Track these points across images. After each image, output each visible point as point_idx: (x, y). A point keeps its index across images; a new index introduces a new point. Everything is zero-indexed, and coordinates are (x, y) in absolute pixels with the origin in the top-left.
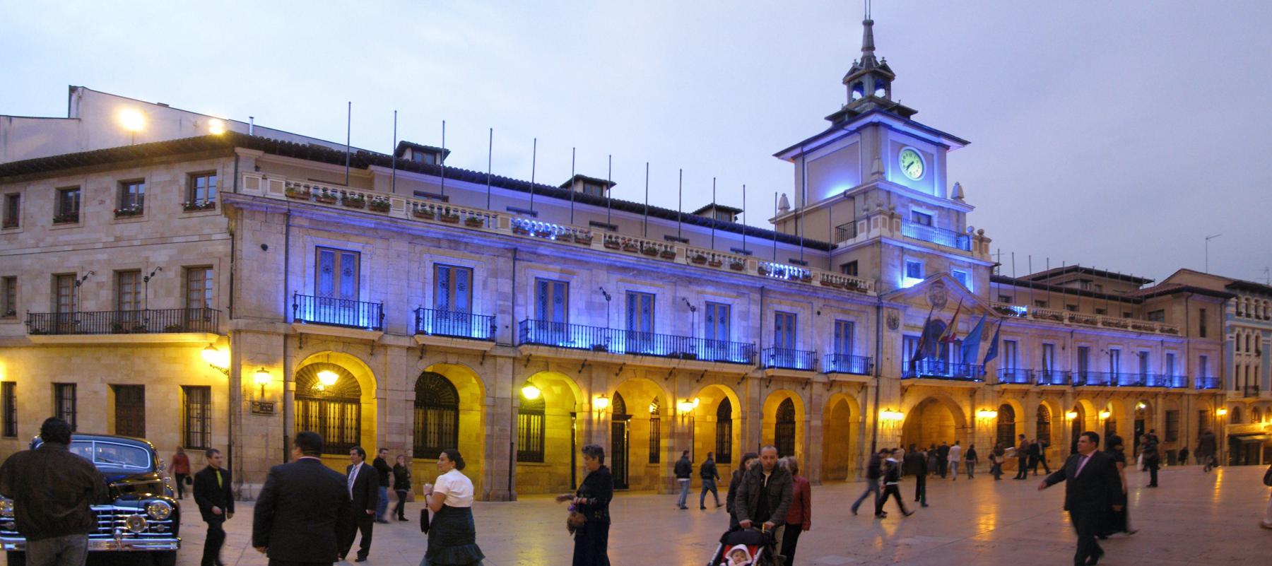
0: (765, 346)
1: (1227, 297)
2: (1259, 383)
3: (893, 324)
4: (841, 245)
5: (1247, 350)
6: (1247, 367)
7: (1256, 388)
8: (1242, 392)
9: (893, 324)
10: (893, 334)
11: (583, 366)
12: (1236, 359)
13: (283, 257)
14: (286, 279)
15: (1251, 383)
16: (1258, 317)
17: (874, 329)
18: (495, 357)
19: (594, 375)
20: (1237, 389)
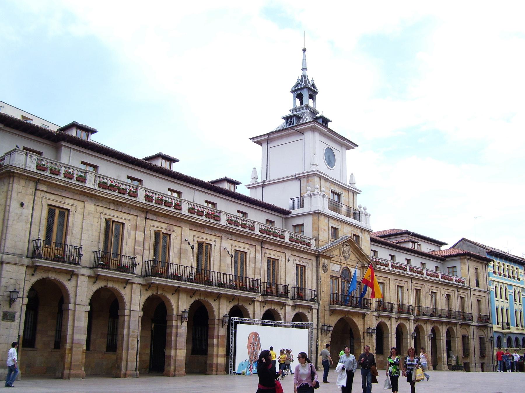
0: (262, 281)
1: (489, 261)
2: (510, 321)
3: (325, 270)
4: (294, 212)
5: (501, 298)
6: (502, 309)
7: (508, 324)
8: (501, 326)
9: (325, 270)
12: (496, 303)
14: (30, 228)
16: (505, 276)
17: (315, 269)
18: (132, 283)
19: (180, 296)
20: (498, 324)
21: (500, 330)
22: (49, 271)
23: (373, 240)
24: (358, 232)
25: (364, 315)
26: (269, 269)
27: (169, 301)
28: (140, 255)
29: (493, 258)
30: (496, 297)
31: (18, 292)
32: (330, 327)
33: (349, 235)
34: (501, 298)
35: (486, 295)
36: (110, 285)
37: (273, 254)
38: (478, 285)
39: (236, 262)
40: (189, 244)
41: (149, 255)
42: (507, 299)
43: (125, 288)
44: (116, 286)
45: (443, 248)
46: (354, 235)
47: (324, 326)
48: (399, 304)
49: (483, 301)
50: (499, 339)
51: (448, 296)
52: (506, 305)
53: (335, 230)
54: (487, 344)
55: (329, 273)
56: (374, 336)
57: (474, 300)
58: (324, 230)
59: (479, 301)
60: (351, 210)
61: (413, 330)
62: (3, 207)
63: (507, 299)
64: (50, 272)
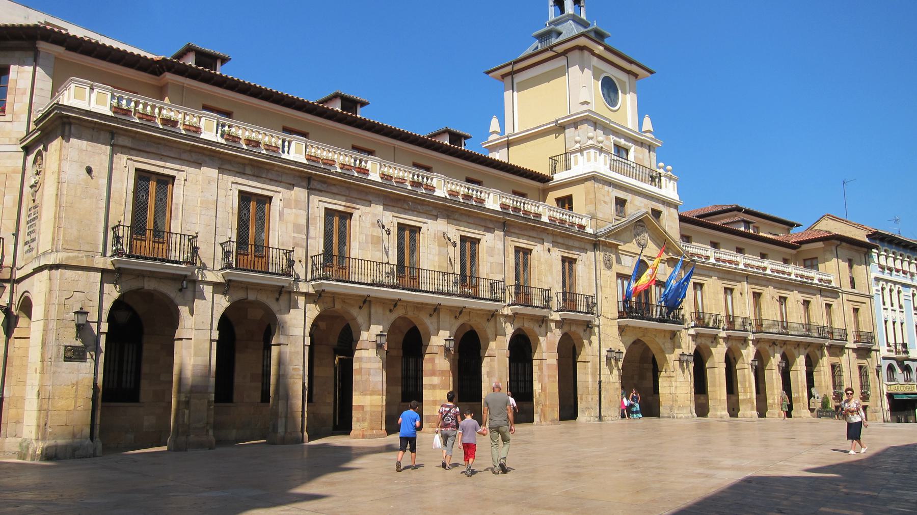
5: (892, 305)
6: (894, 323)
7: (904, 345)
8: (893, 348)
10: (608, 272)
11: (365, 302)
13: (105, 181)
15: (899, 341)
19: (373, 311)
20: (888, 345)
21: (893, 355)
22: (143, 276)
23: (682, 219)
24: (660, 207)
25: (674, 335)
26: (517, 264)
27: (354, 319)
28: (302, 247)
29: (877, 243)
30: (884, 304)
31: (86, 313)
32: (620, 352)
33: (644, 210)
34: (892, 305)
35: (867, 300)
36: (252, 296)
37: (523, 243)
38: (853, 286)
39: (463, 255)
40: (383, 227)
41: (317, 246)
42: (901, 307)
43: (277, 300)
44: (263, 298)
45: (794, 230)
46: (653, 210)
47: (610, 351)
48: (728, 316)
49: (863, 309)
50: (891, 368)
51: (806, 303)
52: (899, 317)
53: (621, 203)
54: (872, 376)
55: (616, 268)
56: (692, 365)
57: (849, 307)
58: (605, 202)
59: (856, 310)
60: (647, 171)
61: (752, 357)
62: (56, 175)
63: (901, 307)
64: (146, 279)
